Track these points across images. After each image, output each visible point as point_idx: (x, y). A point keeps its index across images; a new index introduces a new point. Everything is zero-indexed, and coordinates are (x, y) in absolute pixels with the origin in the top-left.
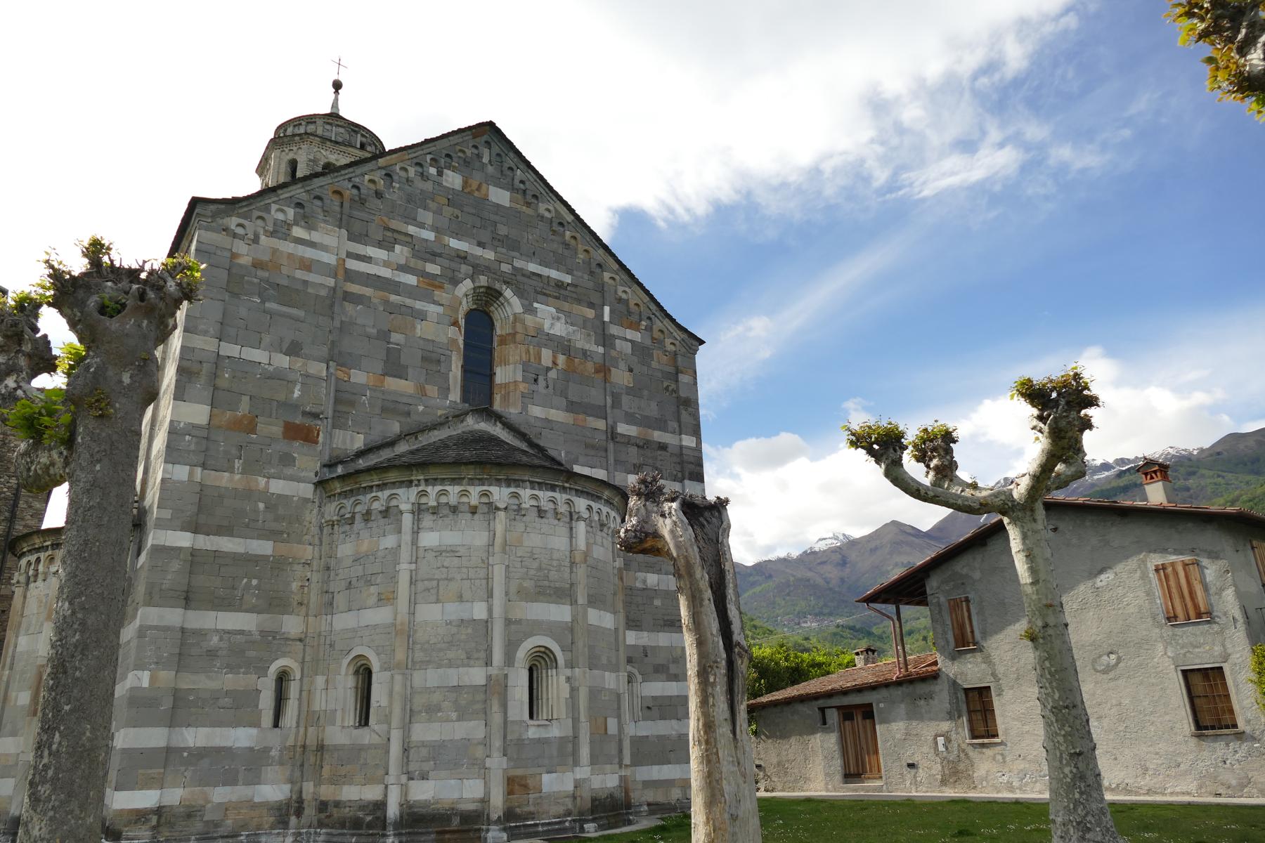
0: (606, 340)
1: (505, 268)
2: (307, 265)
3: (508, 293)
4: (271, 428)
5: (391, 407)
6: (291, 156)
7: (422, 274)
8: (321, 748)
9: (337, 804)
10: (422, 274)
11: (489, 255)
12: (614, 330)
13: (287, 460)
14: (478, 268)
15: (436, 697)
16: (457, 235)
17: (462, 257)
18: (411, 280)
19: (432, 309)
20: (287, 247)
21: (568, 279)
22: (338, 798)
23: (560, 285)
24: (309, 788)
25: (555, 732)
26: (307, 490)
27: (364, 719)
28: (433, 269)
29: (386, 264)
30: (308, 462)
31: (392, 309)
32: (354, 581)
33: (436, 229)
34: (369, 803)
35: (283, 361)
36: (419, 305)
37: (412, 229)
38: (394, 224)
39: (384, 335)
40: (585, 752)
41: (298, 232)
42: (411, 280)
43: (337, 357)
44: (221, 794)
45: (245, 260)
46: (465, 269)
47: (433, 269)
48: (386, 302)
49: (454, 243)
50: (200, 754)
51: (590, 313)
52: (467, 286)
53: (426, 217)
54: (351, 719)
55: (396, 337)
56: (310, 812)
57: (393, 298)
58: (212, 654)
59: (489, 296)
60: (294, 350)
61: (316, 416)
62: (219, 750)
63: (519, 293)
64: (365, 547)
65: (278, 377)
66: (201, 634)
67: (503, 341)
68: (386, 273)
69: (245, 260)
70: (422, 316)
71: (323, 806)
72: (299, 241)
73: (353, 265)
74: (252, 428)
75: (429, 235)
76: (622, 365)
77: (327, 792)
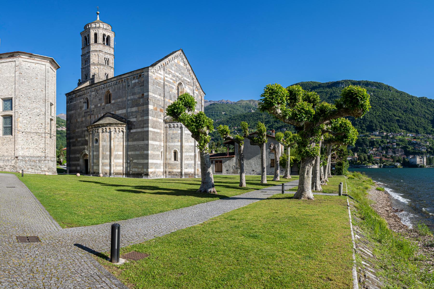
2: (161, 79)
7: (173, 80)
9: (172, 172)
10: (173, 80)
11: (180, 76)
13: (160, 115)
14: (180, 79)
15: (188, 157)
16: (177, 72)
19: (175, 87)
20: (158, 75)
21: (189, 81)
27: (175, 160)
28: (174, 79)
31: (170, 87)
35: (159, 97)
36: (173, 86)
37: (172, 71)
38: (170, 70)
42: (172, 81)
44: (157, 170)
45: (154, 78)
50: (155, 164)
51: (192, 88)
52: (178, 82)
54: (173, 159)
55: (171, 92)
58: (155, 148)
59: (180, 84)
60: (160, 95)
62: (157, 163)
64: (175, 132)
66: (154, 145)
68: (169, 80)
69: (154, 78)
70: (173, 88)
71: (169, 172)
72: (160, 74)
77: (171, 170)
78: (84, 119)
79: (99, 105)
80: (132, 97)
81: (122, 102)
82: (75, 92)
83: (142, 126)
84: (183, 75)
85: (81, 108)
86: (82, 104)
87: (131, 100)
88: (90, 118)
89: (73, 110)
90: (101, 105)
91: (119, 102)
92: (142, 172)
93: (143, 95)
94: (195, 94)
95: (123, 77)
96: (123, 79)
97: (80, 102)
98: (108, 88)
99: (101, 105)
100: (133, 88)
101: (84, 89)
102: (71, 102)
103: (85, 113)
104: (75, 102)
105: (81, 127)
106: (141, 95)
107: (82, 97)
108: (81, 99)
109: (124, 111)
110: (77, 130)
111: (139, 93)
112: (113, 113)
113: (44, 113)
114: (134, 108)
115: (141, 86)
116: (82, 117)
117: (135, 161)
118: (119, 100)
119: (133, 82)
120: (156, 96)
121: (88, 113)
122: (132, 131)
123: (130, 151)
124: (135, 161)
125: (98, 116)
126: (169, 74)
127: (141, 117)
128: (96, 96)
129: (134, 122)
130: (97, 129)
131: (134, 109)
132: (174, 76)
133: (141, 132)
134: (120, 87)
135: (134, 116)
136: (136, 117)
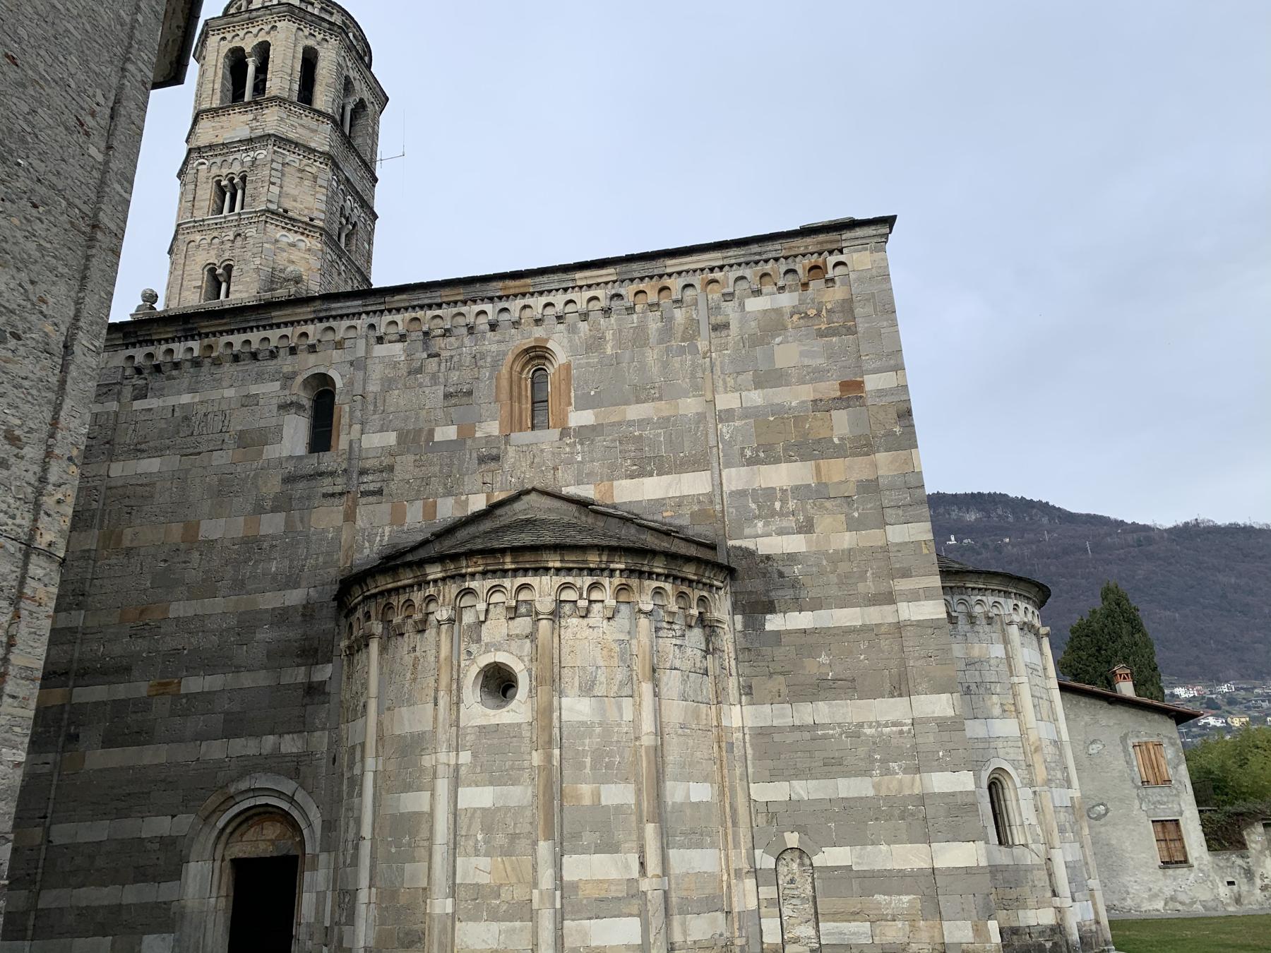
6: (311, 42)
22: (1015, 924)
32: (973, 687)
34: (1046, 927)
78: (272, 524)
79: (447, 433)
80: (756, 398)
81: (665, 422)
82: (205, 326)
83: (869, 586)
85: (252, 441)
86: (266, 416)
87: (747, 413)
89: (158, 452)
90: (466, 433)
95: (672, 265)
96: (675, 284)
97: (249, 401)
98: (539, 332)
101: (304, 312)
102: (141, 394)
104: (186, 399)
105: (239, 586)
106: (830, 388)
107: (272, 365)
108: (260, 378)
109: (694, 484)
110: (179, 609)
111: (817, 375)
112: (587, 491)
113: (57, 339)
114: (784, 466)
115: (821, 334)
116: (259, 509)
117: (833, 856)
119: (755, 305)
121: (326, 485)
122: (774, 623)
123: (773, 776)
124: (833, 856)
125: (430, 511)
129: (792, 558)
130: (509, 583)
131: (781, 475)
133: (865, 629)
134: (641, 329)
135: (790, 522)
136: (806, 528)
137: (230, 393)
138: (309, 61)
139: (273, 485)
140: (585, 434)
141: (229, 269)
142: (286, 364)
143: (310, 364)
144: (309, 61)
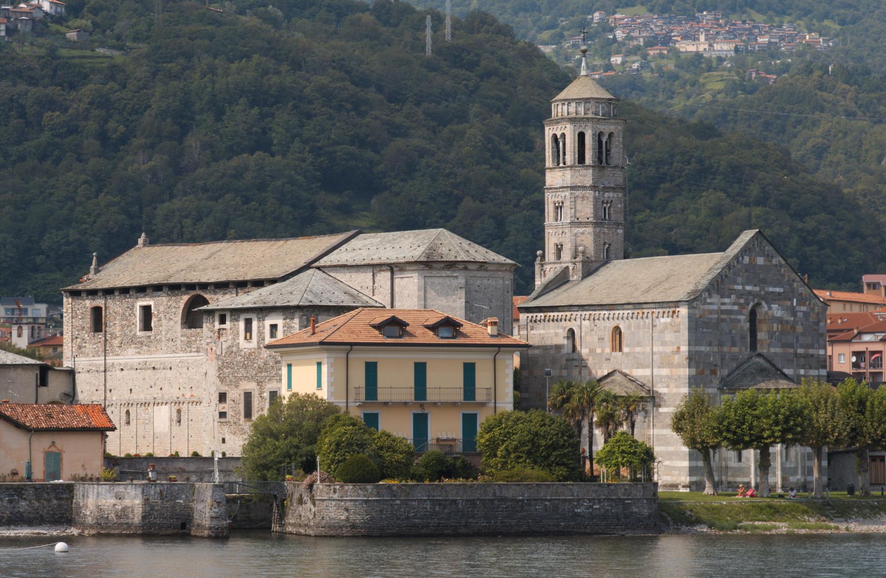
0: (794, 313)
1: (763, 293)
2: (711, 312)
3: (763, 303)
4: (707, 372)
5: (734, 358)
6: (581, 130)
8: (727, 467)
11: (757, 289)
12: (798, 309)
13: (711, 381)
17: (750, 293)
18: (736, 308)
20: (707, 307)
21: (782, 290)
23: (779, 294)
24: (724, 478)
25: (793, 465)
26: (715, 390)
29: (730, 304)
30: (716, 382)
31: (733, 321)
33: (743, 284)
35: (708, 349)
39: (730, 332)
40: (800, 471)
41: (709, 300)
42: (736, 308)
43: (721, 344)
46: (751, 297)
47: (742, 301)
48: (730, 319)
49: (748, 288)
51: (789, 303)
53: (739, 280)
56: (725, 484)
57: (732, 317)
60: (710, 344)
61: (716, 365)
63: (767, 303)
65: (707, 355)
67: (760, 322)
68: (729, 307)
71: (729, 483)
73: (723, 307)
74: (703, 373)
75: (740, 287)
76: (800, 323)
77: (730, 479)
78: (565, 373)
81: (643, 353)
84: (765, 283)
87: (660, 353)
88: (580, 373)
90: (603, 351)
91: (639, 353)
92: (678, 482)
93: (679, 348)
94: (800, 315)
99: (603, 351)
100: (662, 332)
102: (532, 329)
103: (567, 360)
104: (542, 332)
108: (558, 327)
109: (647, 372)
116: (561, 369)
118: (638, 349)
119: (662, 320)
120: (702, 348)
126: (729, 297)
127: (677, 387)
128: (592, 330)
132: (740, 295)
134: (639, 324)
136: (668, 386)
137: (552, 331)
138: (581, 136)
139: (564, 362)
140: (628, 354)
141: (562, 245)
142: (563, 323)
143: (569, 325)
144: (581, 136)
